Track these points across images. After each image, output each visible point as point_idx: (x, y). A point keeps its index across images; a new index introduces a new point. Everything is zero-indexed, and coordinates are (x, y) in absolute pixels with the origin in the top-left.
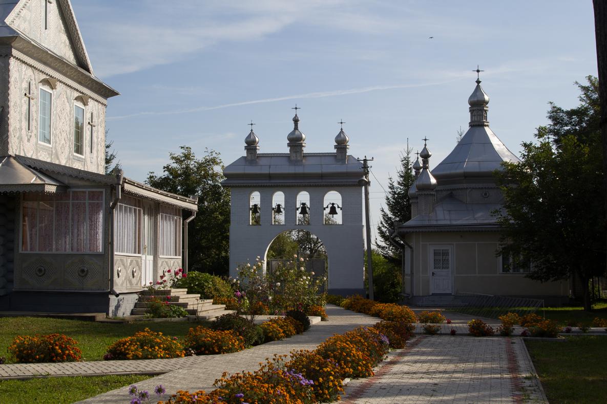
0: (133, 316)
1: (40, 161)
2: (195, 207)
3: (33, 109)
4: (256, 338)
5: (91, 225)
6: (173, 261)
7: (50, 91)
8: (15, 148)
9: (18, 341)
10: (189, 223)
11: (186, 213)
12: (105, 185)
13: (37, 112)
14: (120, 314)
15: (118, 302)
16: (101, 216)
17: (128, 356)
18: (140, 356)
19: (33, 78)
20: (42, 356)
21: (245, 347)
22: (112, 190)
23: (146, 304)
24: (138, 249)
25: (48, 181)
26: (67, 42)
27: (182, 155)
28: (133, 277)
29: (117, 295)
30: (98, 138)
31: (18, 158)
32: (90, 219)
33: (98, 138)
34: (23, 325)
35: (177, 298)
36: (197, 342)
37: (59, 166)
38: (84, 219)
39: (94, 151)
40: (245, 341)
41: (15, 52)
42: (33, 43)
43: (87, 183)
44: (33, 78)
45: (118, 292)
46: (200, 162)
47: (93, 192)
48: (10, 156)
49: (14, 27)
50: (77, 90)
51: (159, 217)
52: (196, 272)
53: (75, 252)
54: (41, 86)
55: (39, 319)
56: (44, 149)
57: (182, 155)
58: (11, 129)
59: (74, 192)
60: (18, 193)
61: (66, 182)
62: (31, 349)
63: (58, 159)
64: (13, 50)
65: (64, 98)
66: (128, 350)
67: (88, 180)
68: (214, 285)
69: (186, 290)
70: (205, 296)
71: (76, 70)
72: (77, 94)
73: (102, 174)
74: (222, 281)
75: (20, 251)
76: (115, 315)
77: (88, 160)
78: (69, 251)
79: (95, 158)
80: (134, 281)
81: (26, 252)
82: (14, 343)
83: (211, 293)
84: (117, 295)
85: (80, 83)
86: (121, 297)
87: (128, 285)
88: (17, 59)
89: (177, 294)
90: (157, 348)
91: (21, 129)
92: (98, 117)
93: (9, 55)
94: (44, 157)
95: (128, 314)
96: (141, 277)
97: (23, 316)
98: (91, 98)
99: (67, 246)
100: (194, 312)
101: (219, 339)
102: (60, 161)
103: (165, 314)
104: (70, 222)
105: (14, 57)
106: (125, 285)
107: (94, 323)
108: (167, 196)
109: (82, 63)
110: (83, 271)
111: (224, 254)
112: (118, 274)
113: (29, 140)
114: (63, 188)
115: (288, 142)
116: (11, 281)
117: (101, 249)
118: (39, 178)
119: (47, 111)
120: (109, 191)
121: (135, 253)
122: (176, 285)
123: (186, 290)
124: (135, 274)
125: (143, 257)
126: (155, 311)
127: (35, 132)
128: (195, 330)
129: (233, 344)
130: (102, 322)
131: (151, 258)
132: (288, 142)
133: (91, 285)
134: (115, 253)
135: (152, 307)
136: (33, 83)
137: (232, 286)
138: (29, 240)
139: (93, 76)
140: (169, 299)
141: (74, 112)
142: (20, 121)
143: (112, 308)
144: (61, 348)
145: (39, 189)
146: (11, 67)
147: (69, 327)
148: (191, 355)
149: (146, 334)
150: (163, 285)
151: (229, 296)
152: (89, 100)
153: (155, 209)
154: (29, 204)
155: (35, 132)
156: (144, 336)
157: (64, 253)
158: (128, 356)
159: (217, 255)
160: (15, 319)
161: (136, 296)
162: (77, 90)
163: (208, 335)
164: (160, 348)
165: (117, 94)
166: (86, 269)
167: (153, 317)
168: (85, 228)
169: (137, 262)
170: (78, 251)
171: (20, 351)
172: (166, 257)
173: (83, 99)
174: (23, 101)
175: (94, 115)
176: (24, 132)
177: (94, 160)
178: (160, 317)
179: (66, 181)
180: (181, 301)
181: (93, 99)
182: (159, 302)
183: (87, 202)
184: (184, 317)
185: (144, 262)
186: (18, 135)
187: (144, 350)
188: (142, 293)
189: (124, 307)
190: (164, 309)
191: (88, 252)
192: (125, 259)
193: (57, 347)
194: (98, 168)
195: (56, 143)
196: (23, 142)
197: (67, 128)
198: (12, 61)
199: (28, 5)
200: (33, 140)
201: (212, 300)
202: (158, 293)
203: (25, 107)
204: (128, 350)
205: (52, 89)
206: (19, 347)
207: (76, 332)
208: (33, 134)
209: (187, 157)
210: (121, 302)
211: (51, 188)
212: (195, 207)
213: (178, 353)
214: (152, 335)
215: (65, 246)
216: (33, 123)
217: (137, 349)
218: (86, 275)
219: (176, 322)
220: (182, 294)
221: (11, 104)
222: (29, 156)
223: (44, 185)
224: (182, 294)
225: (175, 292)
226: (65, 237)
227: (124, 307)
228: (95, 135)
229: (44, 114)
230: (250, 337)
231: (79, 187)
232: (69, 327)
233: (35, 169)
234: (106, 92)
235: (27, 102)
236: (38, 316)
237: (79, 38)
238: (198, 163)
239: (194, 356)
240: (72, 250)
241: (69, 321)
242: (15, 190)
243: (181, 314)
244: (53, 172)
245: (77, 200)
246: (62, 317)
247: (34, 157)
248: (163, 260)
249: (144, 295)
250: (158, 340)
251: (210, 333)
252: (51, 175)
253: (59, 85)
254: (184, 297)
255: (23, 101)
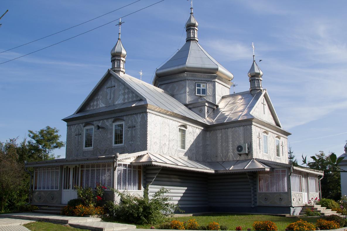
0: (300, 215)
1: (264, 160)
2: (323, 174)
3: (261, 142)
4: (344, 224)
5: (282, 182)
6: (315, 194)
7: (267, 135)
8: (255, 156)
9: (255, 223)
10: (321, 180)
11: (320, 176)
12: (287, 168)
13: (262, 143)
14: (295, 215)
15: (294, 210)
16: (286, 179)
17: (294, 229)
18: (298, 230)
19: (260, 131)
20: (263, 228)
21: (340, 227)
22: (289, 170)
23: (305, 211)
24: (301, 190)
25: (266, 167)
26: (272, 117)
27: (320, 154)
28: (300, 200)
29: (293, 208)
30: (285, 150)
31: (256, 159)
32: (282, 180)
33: (285, 150)
34: (260, 218)
35: (317, 209)
36: (320, 225)
37: (271, 162)
38: (280, 180)
39: (284, 155)
40: (340, 225)
41: (253, 123)
42: (259, 119)
43: (280, 167)
44: (260, 131)
45: (293, 206)
46: (327, 156)
47: (283, 170)
48: (254, 159)
49: (253, 115)
50: (276, 134)
51: (309, 178)
52: (325, 199)
53: (277, 192)
54: (263, 134)
55: (266, 216)
56: (265, 155)
57: (320, 154)
58: (253, 149)
59: (276, 170)
60: (256, 171)
61: (273, 167)
62: (260, 226)
63: (271, 159)
64: (253, 122)
65: (272, 137)
66: (294, 227)
67: (280, 166)
68: (332, 203)
69: (321, 205)
70: (328, 208)
71: (275, 127)
72: (276, 135)
73: (287, 164)
74: (335, 202)
75: (259, 192)
76: (293, 215)
77: (282, 158)
78: (275, 191)
79: (284, 158)
80: (300, 202)
81: (269, 192)
82: (254, 224)
83: (330, 206)
84: (293, 208)
85: (277, 132)
86: (294, 208)
87: (298, 204)
88: (254, 125)
89: (316, 207)
90: (304, 227)
91: (257, 149)
92: (285, 143)
93: (252, 124)
94: (266, 158)
95: (298, 214)
96: (302, 201)
97: (261, 215)
98: (281, 136)
99: (275, 190)
100: (323, 214)
101: (329, 224)
102: (271, 159)
103: (312, 214)
104: (275, 181)
105: (253, 125)
106: (296, 204)
107: (285, 218)
108: (311, 170)
109: (278, 125)
110: (280, 199)
111: (339, 192)
112: (293, 200)
113: (260, 153)
114: (272, 169)
115: (345, 149)
116: (256, 202)
117: (286, 191)
118: (263, 166)
119: (266, 142)
120: (288, 170)
121: (300, 192)
122: (317, 204)
123: (321, 205)
124: (300, 200)
125: (303, 193)
126: (308, 213)
127: (262, 149)
128: (320, 221)
129: (335, 226)
130: (288, 217)
131: (306, 193)
132: (345, 149)
133: (283, 204)
134: (292, 192)
135: (307, 212)
136: (260, 133)
137: (339, 204)
138: (262, 187)
139: (282, 129)
140: (313, 209)
141: (275, 142)
142: (257, 146)
143: (292, 212)
144: (270, 226)
145: (264, 170)
146: (252, 128)
147: (276, 219)
148: (318, 230)
149: (301, 221)
150: (310, 204)
151: (338, 208)
152: (281, 137)
153: (306, 175)
154: (260, 175)
155: (262, 149)
156: (300, 222)
157: (273, 192)
158: (294, 229)
159: (336, 192)
160: (257, 216)
161: (301, 208)
162: (276, 134)
163: (325, 222)
164: (306, 227)
165: (291, 134)
166: (281, 198)
167: (307, 216)
168: (281, 182)
169: (301, 195)
170: (278, 191)
171: (256, 226)
172: (313, 193)
173: (278, 137)
174: (257, 139)
175: (283, 142)
176: (258, 150)
177: (284, 158)
178: (310, 216)
179: (273, 166)
180: (318, 210)
181: (282, 137)
182: (309, 210)
183: (275, 174)
184: (319, 215)
185: (304, 195)
186: (256, 151)
187: (299, 227)
188: (303, 207)
189: (296, 212)
190: (311, 213)
191: (282, 192)
192: (296, 194)
193: (268, 226)
194: (286, 162)
195: (270, 153)
196: (258, 153)
197: (273, 147)
198: (253, 126)
199: (257, 107)
200: (261, 153)
201: (331, 209)
202: (309, 206)
203: (258, 142)
204: (294, 227)
205: (267, 134)
206: (255, 225)
207: (278, 221)
208: (261, 151)
209: (322, 155)
210: (295, 210)
211: (267, 169)
212: (323, 174)
213: (313, 229)
214: (303, 222)
215: (274, 189)
216: (261, 147)
217: (297, 227)
218: (282, 200)
219: (316, 218)
220: (319, 207)
221: (253, 141)
222: (260, 158)
223: (265, 168)
224: (319, 207)
225: (316, 206)
226: (274, 187)
227: (296, 212)
228: (284, 149)
229: (265, 143)
230: (342, 223)
231: (277, 168)
232: (276, 219)
233: (262, 163)
234: (287, 134)
235: (259, 140)
236: (265, 215)
237: (276, 116)
238: (326, 157)
239: (319, 230)
240: (276, 191)
241: (276, 217)
242: (255, 170)
243: (318, 215)
244: (268, 163)
245: (277, 173)
246: (274, 215)
247: (262, 159)
248: (311, 194)
249: (304, 207)
250: (305, 224)
251: (326, 221)
252: (268, 165)
253: (269, 133)
254: (319, 208)
255: (257, 139)
